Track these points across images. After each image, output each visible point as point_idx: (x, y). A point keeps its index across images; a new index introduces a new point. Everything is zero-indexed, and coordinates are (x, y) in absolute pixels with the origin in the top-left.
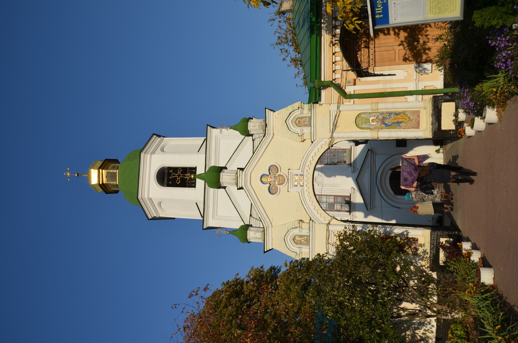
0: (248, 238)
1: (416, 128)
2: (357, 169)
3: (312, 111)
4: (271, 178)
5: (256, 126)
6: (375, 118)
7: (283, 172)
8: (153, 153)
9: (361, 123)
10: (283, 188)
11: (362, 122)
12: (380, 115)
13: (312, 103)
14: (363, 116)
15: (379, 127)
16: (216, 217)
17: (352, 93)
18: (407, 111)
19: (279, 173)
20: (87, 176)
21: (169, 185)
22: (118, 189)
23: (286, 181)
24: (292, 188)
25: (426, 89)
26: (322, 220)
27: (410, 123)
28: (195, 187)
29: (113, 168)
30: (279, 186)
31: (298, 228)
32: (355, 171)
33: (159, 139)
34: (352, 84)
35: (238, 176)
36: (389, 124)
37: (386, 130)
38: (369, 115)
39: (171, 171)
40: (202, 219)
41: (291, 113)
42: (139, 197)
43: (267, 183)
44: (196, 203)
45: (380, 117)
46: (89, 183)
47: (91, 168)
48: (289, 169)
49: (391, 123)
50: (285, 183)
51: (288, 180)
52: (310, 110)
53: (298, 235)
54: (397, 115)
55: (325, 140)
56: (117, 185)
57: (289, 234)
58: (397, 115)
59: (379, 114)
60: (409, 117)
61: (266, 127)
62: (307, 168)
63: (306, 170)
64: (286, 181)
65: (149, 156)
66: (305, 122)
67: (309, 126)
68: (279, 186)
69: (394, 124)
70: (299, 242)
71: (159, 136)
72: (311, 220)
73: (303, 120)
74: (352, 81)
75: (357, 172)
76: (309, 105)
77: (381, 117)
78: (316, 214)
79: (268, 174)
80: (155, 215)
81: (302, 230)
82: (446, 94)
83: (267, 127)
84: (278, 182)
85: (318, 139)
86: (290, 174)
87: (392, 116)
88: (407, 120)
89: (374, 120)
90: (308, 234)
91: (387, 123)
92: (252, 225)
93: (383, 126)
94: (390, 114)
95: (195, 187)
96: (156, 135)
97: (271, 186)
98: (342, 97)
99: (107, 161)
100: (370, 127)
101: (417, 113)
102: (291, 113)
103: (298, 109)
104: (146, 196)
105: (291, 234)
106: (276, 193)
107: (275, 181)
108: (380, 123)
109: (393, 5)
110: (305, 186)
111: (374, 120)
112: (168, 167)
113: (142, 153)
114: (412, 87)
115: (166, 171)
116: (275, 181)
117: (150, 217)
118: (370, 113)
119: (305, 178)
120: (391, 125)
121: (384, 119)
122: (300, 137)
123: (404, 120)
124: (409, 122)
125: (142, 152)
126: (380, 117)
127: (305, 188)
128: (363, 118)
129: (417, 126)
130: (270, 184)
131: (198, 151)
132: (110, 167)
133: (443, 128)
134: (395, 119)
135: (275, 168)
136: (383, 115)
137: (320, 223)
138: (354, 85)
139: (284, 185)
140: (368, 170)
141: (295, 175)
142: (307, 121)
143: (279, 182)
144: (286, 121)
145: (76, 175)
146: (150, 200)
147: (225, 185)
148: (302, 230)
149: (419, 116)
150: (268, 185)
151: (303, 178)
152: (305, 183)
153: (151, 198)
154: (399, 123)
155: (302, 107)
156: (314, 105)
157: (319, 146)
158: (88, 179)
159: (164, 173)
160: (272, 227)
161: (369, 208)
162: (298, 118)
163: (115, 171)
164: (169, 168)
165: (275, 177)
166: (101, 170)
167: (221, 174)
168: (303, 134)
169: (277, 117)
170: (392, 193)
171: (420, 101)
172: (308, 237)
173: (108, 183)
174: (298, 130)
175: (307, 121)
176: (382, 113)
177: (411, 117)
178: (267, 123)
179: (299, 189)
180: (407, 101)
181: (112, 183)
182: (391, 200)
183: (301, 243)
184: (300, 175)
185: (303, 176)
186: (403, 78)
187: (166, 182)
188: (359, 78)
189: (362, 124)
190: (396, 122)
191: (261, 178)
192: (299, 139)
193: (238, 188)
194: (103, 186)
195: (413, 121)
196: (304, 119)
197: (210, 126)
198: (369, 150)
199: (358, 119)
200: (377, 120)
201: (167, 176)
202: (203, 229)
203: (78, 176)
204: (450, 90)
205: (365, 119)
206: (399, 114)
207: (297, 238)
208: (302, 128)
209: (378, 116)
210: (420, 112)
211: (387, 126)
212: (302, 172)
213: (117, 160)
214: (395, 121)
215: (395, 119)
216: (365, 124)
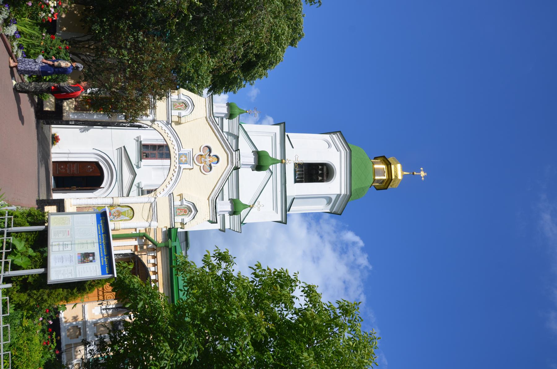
8: (339, 196)
11: (128, 212)
14: (128, 218)
15: (112, 208)
16: (273, 135)
19: (202, 165)
20: (405, 173)
21: (323, 165)
24: (189, 152)
30: (202, 153)
38: (122, 219)
39: (320, 178)
40: (286, 134)
41: (193, 219)
44: (293, 148)
50: (196, 156)
51: (193, 159)
59: (113, 219)
62: (177, 170)
63: (178, 168)
65: (343, 192)
70: (181, 104)
72: (171, 124)
73: (182, 214)
75: (136, 182)
80: (334, 136)
81: (178, 115)
102: (193, 219)
109: (93, 223)
110: (177, 154)
113: (350, 194)
115: (325, 178)
116: (205, 158)
118: (121, 220)
119: (177, 161)
122: (183, 198)
127: (177, 152)
141: (187, 164)
145: (415, 173)
146: (338, 150)
150: (211, 154)
152: (177, 156)
153: (338, 151)
157: (166, 190)
159: (327, 177)
160: (206, 117)
161: (123, 149)
162: (187, 215)
164: (322, 181)
165: (206, 162)
166: (390, 178)
170: (101, 164)
172: (173, 108)
174: (185, 203)
179: (182, 151)
188: (132, 252)
189: (128, 211)
199: (132, 215)
200: (115, 214)
201: (324, 174)
213: (377, 190)
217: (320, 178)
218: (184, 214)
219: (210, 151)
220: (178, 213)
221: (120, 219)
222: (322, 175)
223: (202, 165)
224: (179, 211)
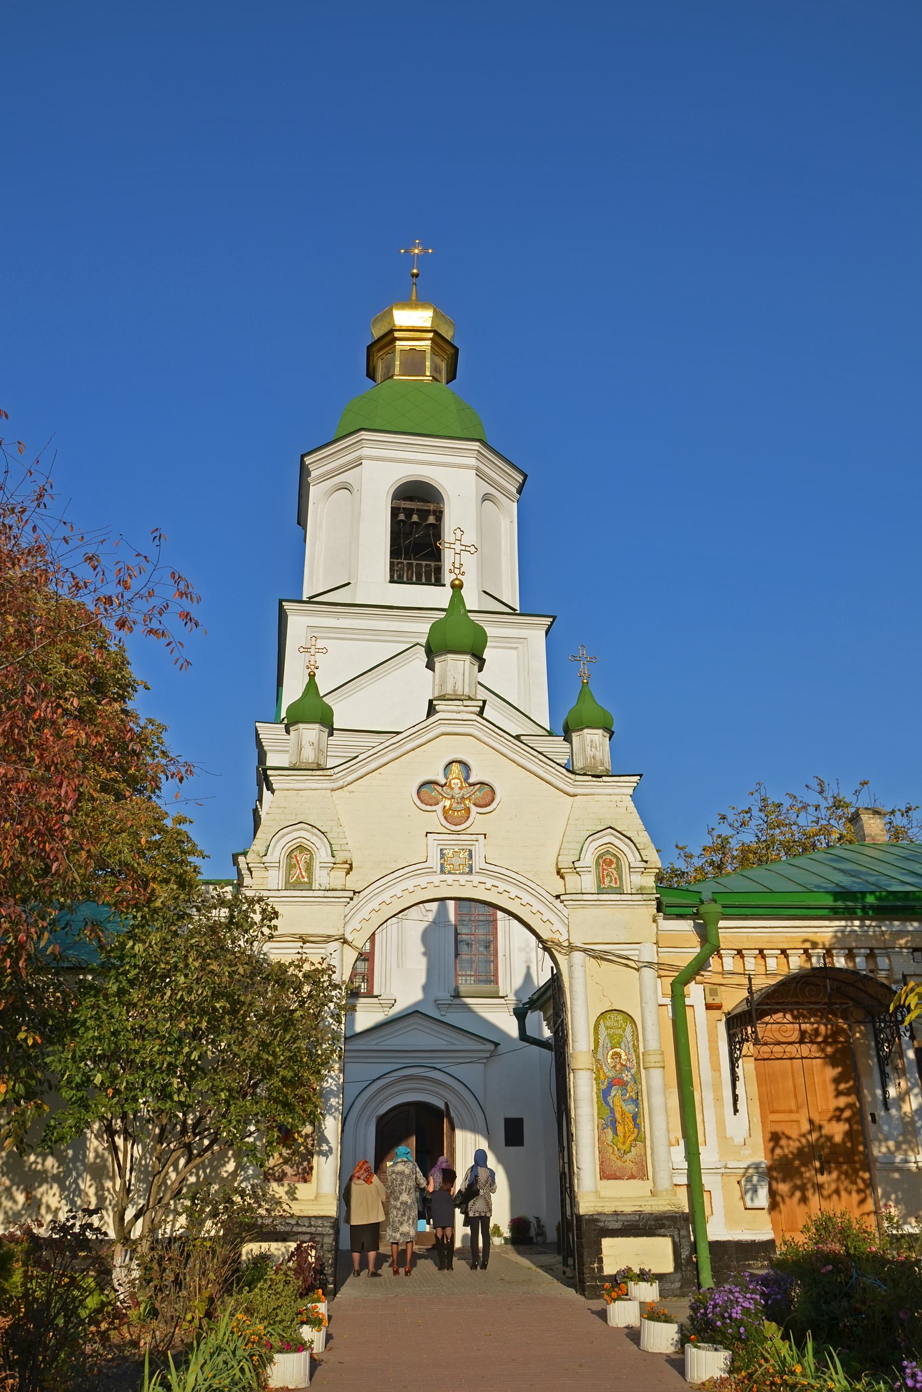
0: (301, 726)
1: (602, 1170)
2: (443, 1013)
3: (639, 897)
4: (461, 788)
5: (593, 749)
6: (624, 1063)
7: (478, 820)
8: (480, 474)
9: (608, 1024)
10: (434, 819)
12: (632, 1075)
13: (658, 896)
14: (629, 1030)
15: (601, 1073)
17: (688, 1001)
18: (645, 1147)
19: (474, 809)
20: (414, 298)
21: (395, 511)
22: (379, 379)
23: (453, 828)
25: (706, 1196)
26: (355, 923)
27: (613, 1153)
28: (390, 582)
29: (436, 369)
31: (333, 860)
32: (439, 1008)
33: (514, 491)
34: (710, 1001)
35: (466, 703)
36: (610, 1099)
37: (595, 1090)
38: (630, 1045)
39: (431, 519)
40: (305, 599)
41: (632, 841)
42: (364, 435)
43: (446, 777)
44: (349, 584)
45: (627, 1076)
46: (396, 305)
47: (435, 311)
48: (485, 835)
49: (611, 1104)
51: (458, 833)
52: (639, 892)
53: (311, 858)
54: (635, 1117)
55: (564, 930)
56: (393, 376)
57: (316, 836)
58: (635, 1117)
59: (633, 1071)
60: (630, 1151)
61: (593, 776)
62: (490, 882)
64: (453, 828)
65: (473, 462)
66: (609, 878)
67: (599, 887)
68: (439, 808)
69: (611, 1113)
70: (294, 861)
71: (519, 491)
72: (355, 893)
73: (615, 872)
74: (717, 1001)
76: (652, 888)
77: (627, 1076)
78: (369, 907)
79: (471, 781)
81: (326, 871)
82: (694, 1247)
83: (594, 779)
84: (451, 805)
85: (566, 912)
86: (474, 837)
87: (629, 1107)
88: (620, 1146)
89: (618, 1060)
90: (315, 886)
91: (613, 1094)
92: (332, 735)
93: (603, 1084)
94: (636, 1101)
95: (392, 581)
96: (524, 481)
97: (439, 788)
98: (676, 974)
99: (453, 351)
100: (600, 1050)
101: (640, 1173)
102: (632, 841)
103: (643, 861)
104: (366, 452)
105: (314, 839)
106: (422, 802)
107: (453, 797)
108: (611, 1074)
110: (443, 877)
111: (618, 1060)
112: (441, 512)
113: (478, 444)
114: (708, 1156)
115: (432, 507)
116: (453, 797)
117: (308, 460)
119: (463, 879)
120: (607, 1104)
121: (623, 1084)
122: (572, 866)
123: (621, 1139)
124: (616, 1152)
125: (481, 443)
126: (627, 1076)
127: (437, 878)
128: (624, 1030)
129: (607, 1174)
130: (445, 784)
131: (485, 592)
132: (438, 360)
133: (607, 1243)
134: (623, 1113)
135: (488, 800)
136: (632, 1083)
137: (345, 916)
138: (706, 1004)
139: (444, 822)
140: (444, 1043)
141: (470, 851)
142: (611, 882)
143: (450, 809)
144: (610, 827)
145: (415, 271)
146: (357, 463)
147: (438, 666)
148: (326, 871)
149: (632, 1177)
151: (463, 873)
152: (449, 878)
153: (361, 464)
154: (613, 1124)
155: (647, 870)
156: (655, 903)
157: (548, 915)
158: (407, 303)
162: (618, 858)
163: (428, 373)
164: (439, 515)
165: (463, 798)
166: (431, 335)
167: (468, 658)
168: (577, 873)
169: (619, 804)
171: (672, 1181)
172: (307, 887)
173: (397, 353)
175: (611, 882)
176: (636, 1080)
177: (628, 1157)
178: (605, 779)
179: (435, 862)
180: (671, 1145)
181: (397, 363)
182: (365, 1106)
183: (290, 867)
184: (471, 867)
185: (467, 873)
186: (729, 1133)
187: (403, 506)
188: (724, 1019)
189: (607, 1028)
190: (614, 1117)
191: (460, 762)
192: (565, 863)
193: (435, 702)
194: (389, 339)
195: (619, 1163)
196: (617, 877)
197: (552, 623)
198: (497, 1044)
199: (620, 1017)
200: (618, 1066)
202: (281, 602)
203: (413, 275)
204: (704, 1257)
205: (621, 1036)
206: (637, 1126)
207: (303, 858)
208: (593, 869)
209: (629, 1069)
210: (643, 1179)
211: (604, 1095)
212: (478, 870)
213: (454, 377)
214: (618, 1116)
215: (623, 1113)
216: (608, 1034)
217: (431, 519)
218: (614, 866)
219: (435, 783)
220: (613, 885)
221: (632, 1051)
222: (424, 514)
223: (474, 809)
224: (607, 880)
